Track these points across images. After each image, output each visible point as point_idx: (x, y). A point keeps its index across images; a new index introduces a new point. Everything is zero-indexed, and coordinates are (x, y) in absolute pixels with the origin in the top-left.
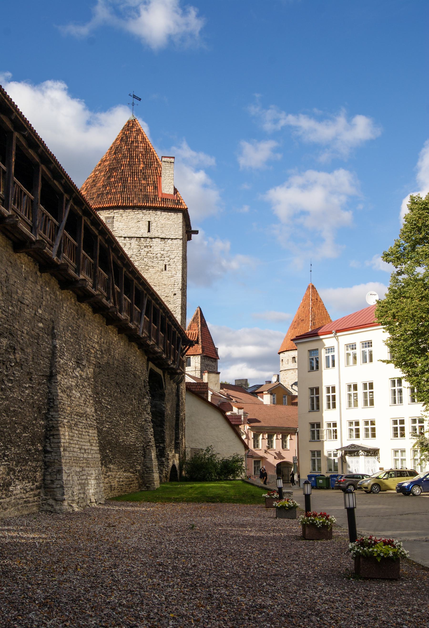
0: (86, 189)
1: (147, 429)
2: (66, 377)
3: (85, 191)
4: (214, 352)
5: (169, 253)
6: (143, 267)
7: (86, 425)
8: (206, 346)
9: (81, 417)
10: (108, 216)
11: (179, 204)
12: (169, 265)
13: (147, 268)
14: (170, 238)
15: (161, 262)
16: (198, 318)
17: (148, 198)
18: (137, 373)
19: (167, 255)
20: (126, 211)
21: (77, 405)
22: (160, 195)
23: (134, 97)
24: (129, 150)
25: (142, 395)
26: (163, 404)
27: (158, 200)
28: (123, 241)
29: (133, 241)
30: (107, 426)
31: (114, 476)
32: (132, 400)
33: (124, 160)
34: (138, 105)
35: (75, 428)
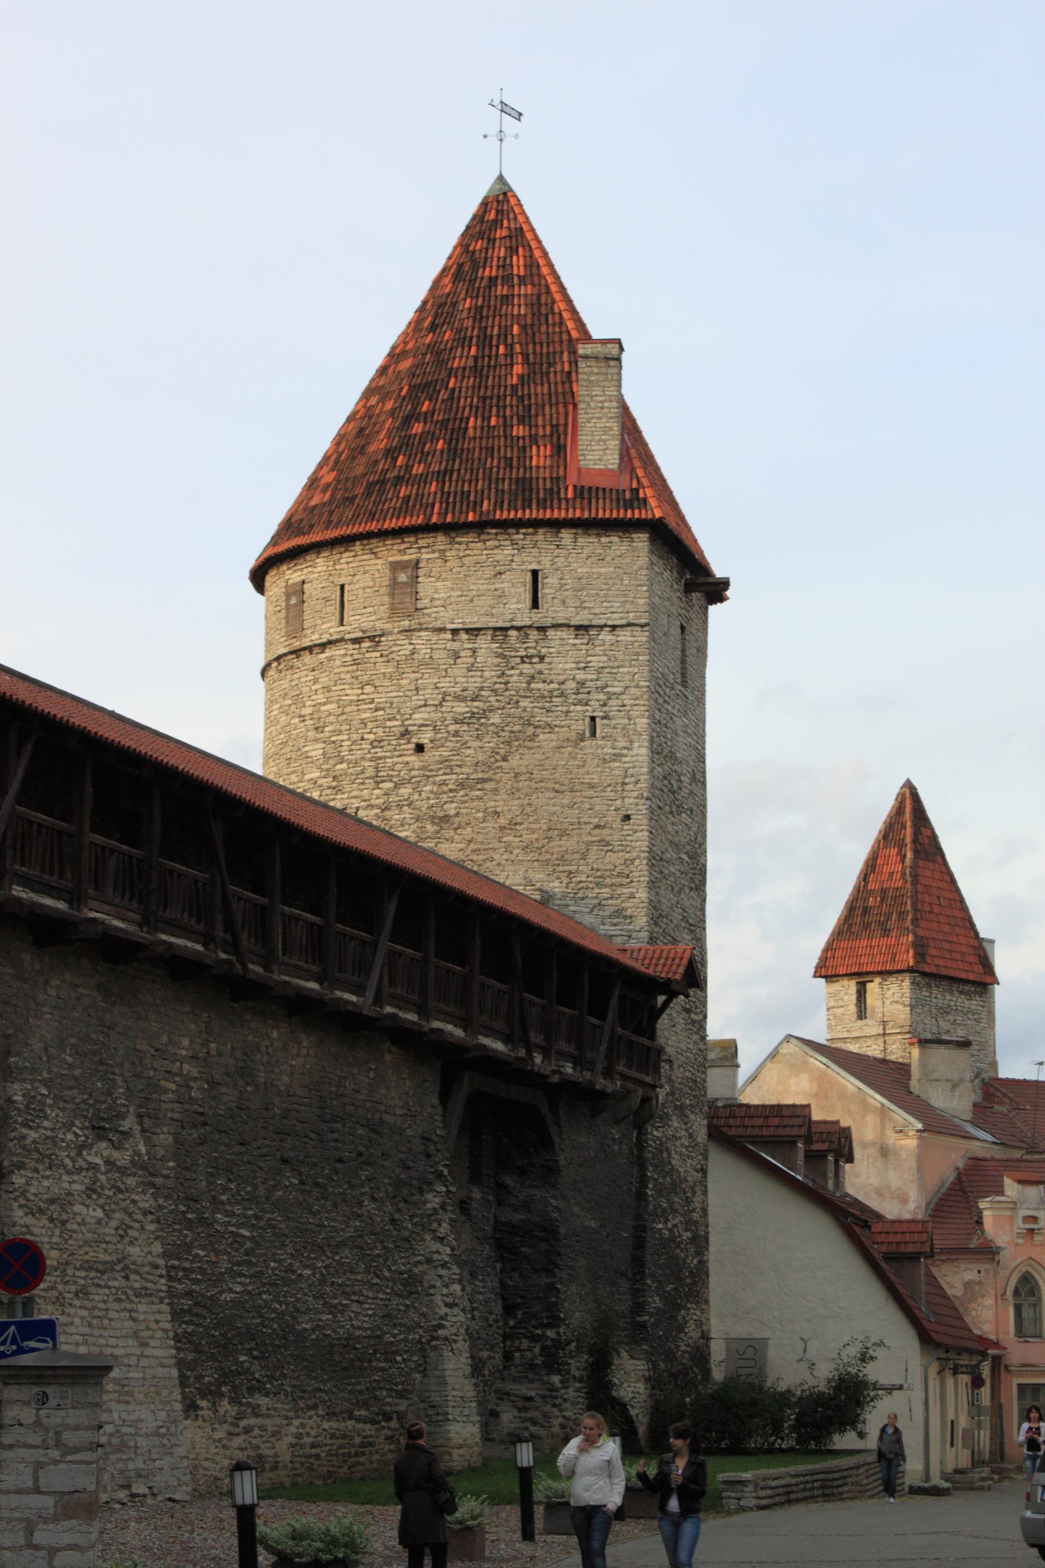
0: (336, 462)
1: (433, 1287)
2: (48, 1173)
3: (333, 469)
4: (971, 959)
5: (605, 677)
6: (517, 728)
7: (125, 1293)
8: (933, 935)
9: (103, 1273)
10: (398, 558)
11: (636, 504)
12: (603, 718)
13: (530, 731)
14: (606, 626)
15: (579, 708)
16: (903, 826)
17: (531, 490)
18: (388, 1118)
19: (599, 684)
20: (458, 539)
21: (87, 1243)
22: (572, 480)
23: (504, 108)
24: (477, 314)
25: (415, 1182)
26: (554, 1197)
27: (562, 495)
28: (450, 645)
29: (483, 642)
30: (239, 1288)
31: (270, 1429)
32: (360, 1204)
33: (458, 354)
34: (517, 136)
35: (76, 1302)
